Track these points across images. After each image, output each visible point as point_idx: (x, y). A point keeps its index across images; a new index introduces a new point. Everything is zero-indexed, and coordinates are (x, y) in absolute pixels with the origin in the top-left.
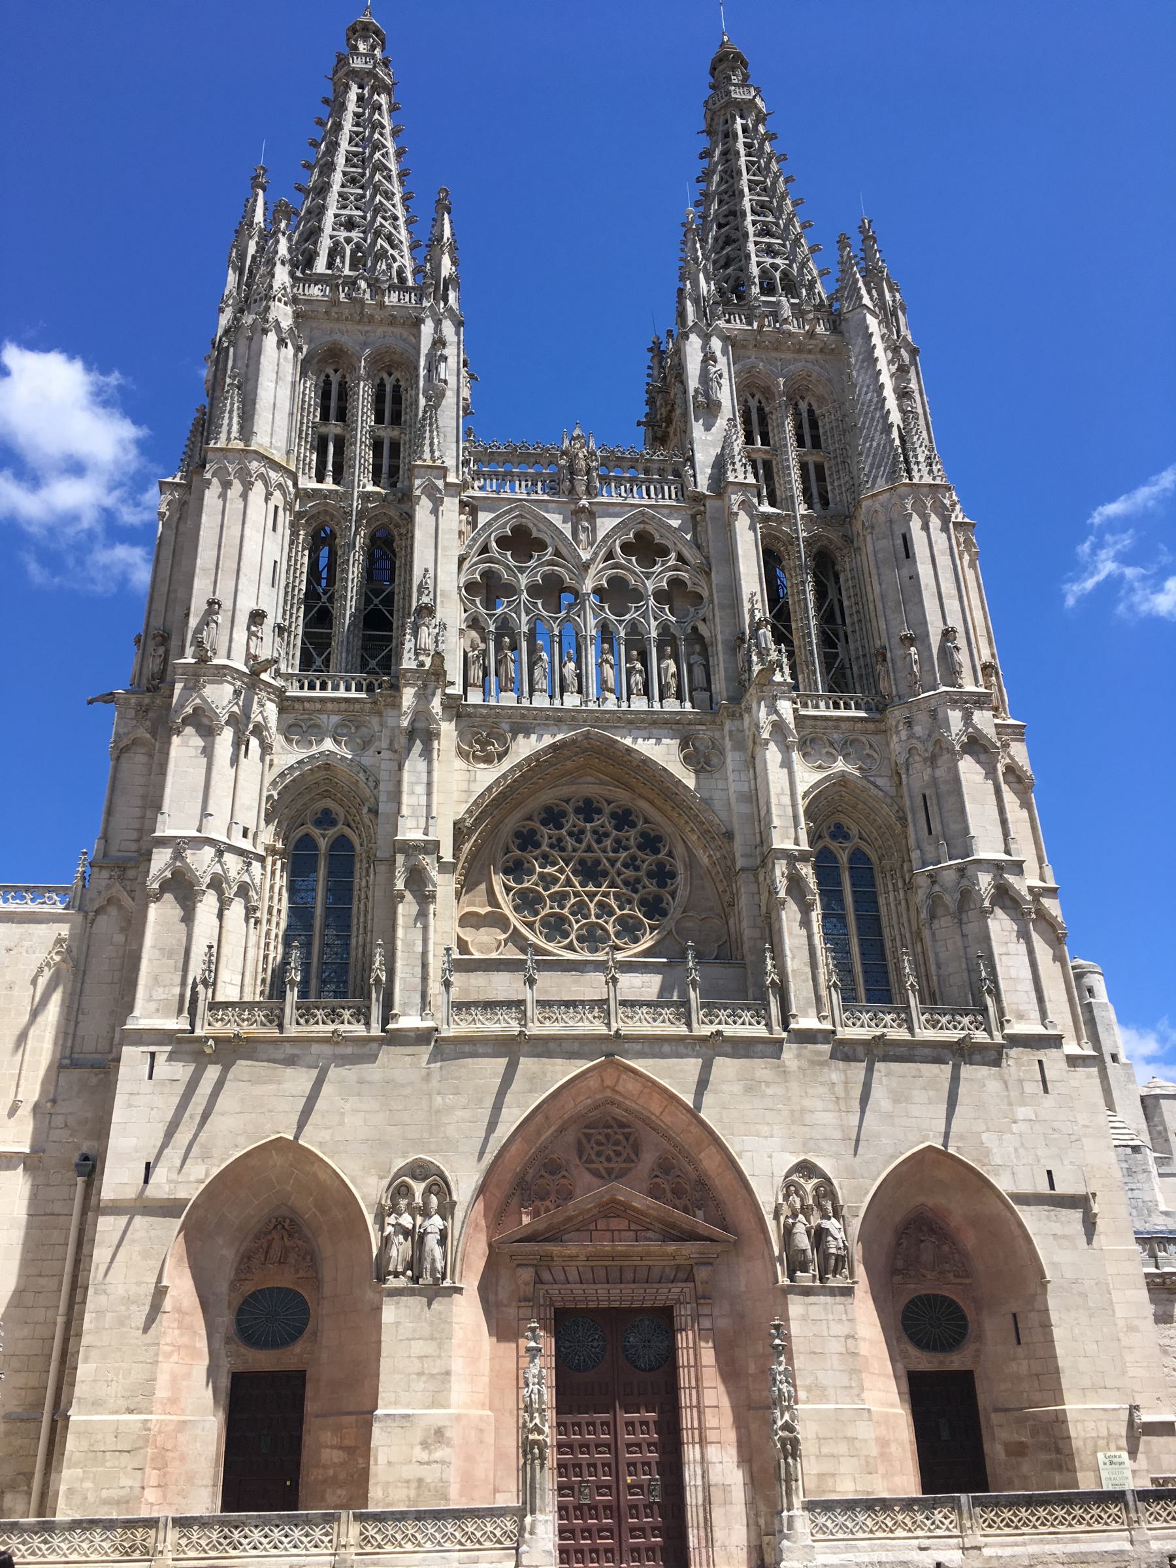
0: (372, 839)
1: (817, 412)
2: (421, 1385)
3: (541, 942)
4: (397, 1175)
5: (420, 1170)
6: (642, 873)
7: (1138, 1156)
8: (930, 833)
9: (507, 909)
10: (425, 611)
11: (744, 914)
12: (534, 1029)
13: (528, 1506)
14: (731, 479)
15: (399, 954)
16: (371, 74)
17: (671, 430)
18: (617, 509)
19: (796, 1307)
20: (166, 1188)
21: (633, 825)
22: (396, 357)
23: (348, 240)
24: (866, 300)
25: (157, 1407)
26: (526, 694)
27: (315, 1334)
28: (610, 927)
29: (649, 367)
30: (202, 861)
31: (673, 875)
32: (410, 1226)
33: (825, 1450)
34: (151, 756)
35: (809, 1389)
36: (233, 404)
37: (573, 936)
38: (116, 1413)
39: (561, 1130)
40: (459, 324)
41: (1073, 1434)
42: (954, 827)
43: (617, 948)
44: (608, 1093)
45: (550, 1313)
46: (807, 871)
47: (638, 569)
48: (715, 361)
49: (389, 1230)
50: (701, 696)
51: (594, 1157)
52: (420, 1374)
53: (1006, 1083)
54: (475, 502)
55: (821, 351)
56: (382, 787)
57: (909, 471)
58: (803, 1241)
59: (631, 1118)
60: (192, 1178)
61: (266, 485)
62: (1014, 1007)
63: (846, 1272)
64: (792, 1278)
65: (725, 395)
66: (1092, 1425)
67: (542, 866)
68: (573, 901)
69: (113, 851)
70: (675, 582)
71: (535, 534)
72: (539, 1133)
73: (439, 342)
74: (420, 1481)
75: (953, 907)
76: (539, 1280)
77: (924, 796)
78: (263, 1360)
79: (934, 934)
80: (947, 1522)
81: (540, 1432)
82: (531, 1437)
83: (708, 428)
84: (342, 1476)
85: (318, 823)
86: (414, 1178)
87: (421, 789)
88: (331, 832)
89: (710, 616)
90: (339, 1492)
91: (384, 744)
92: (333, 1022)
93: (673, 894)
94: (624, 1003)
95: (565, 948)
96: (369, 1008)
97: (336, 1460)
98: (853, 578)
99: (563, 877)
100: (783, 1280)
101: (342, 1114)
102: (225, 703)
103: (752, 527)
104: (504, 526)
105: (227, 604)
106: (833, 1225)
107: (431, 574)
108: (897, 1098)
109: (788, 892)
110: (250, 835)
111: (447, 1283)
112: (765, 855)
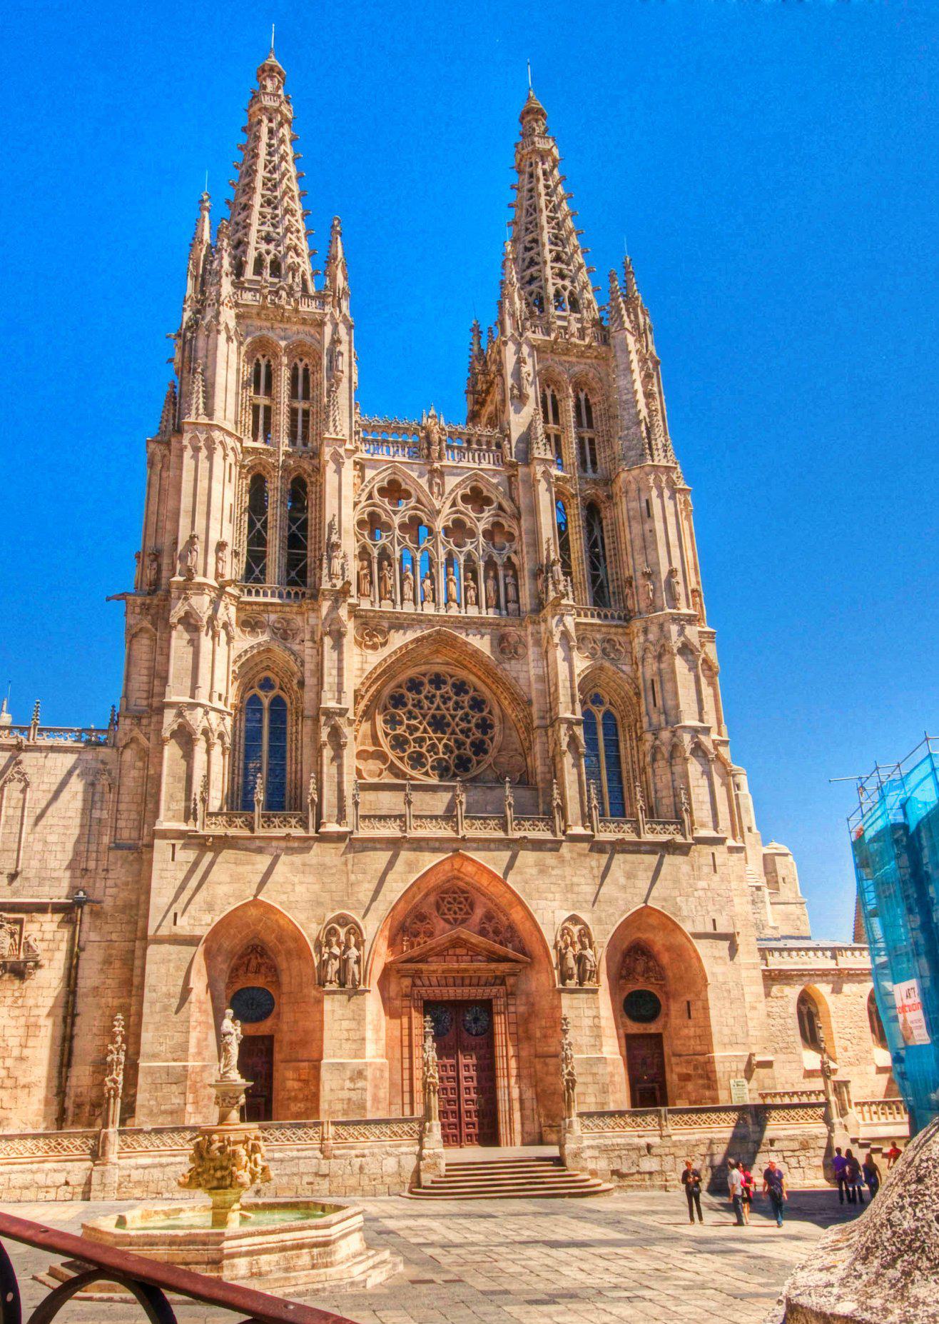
0: (300, 700)
2: (347, 1046)
3: (408, 770)
4: (329, 923)
5: (343, 920)
6: (472, 725)
8: (655, 705)
11: (538, 756)
13: (427, 1116)
14: (536, 456)
15: (325, 784)
16: (278, 110)
17: (489, 399)
18: (459, 471)
19: (566, 1000)
20: (188, 928)
21: (466, 692)
22: (306, 349)
23: (268, 252)
25: (190, 1058)
26: (399, 602)
27: (279, 1014)
29: (471, 344)
30: (197, 719)
31: (491, 727)
36: (198, 386)
37: (428, 767)
38: (167, 1061)
39: (427, 895)
40: (350, 328)
41: (717, 1069)
42: (670, 703)
44: (456, 872)
45: (420, 1003)
46: (579, 731)
47: (473, 515)
49: (326, 956)
51: (446, 911)
52: (347, 1040)
53: (693, 867)
55: (596, 357)
57: (652, 455)
58: (571, 963)
59: (469, 888)
60: (203, 923)
61: (224, 449)
63: (595, 979)
64: (563, 983)
65: (531, 391)
66: (728, 1064)
67: (408, 719)
68: (428, 743)
69: (132, 707)
70: (497, 525)
71: (404, 486)
73: (336, 341)
74: (349, 1099)
75: (666, 755)
76: (414, 985)
77: (652, 681)
79: (654, 771)
81: (434, 1077)
82: (428, 1080)
83: (518, 411)
84: (301, 1096)
85: (262, 687)
86: (339, 924)
87: (335, 672)
88: (272, 694)
91: (307, 637)
93: (492, 739)
95: (423, 774)
96: (307, 818)
98: (612, 524)
99: (422, 727)
100: (559, 986)
101: (293, 885)
102: (205, 609)
103: (549, 490)
104: (383, 480)
106: (589, 953)
107: (336, 519)
108: (630, 876)
109: (569, 745)
110: (223, 699)
111: (362, 987)
112: (552, 721)
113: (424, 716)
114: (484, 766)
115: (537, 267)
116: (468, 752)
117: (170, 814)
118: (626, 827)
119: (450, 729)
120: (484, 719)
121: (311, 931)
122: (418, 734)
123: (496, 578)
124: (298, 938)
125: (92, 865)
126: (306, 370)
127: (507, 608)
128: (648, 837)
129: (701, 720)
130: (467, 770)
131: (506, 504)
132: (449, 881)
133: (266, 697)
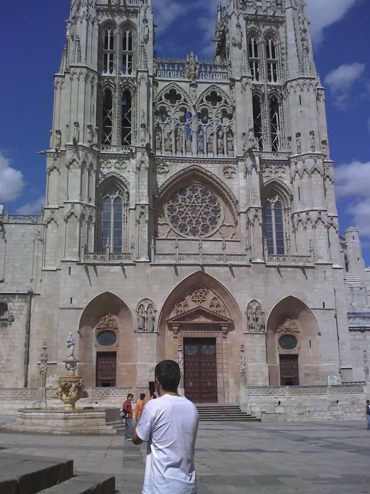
1: (275, 44)
7: (362, 291)
8: (300, 200)
9: (169, 223)
28: (199, 228)
31: (219, 211)
34: (60, 173)
43: (201, 234)
46: (260, 214)
47: (211, 106)
48: (240, 27)
50: (230, 152)
56: (131, 184)
68: (188, 219)
73: (145, 21)
80: (282, 392)
89: (234, 123)
93: (219, 217)
94: (203, 254)
99: (186, 212)
104: (167, 90)
105: (81, 123)
108: (282, 282)
111: (154, 332)
116: (208, 223)
118: (281, 259)
119: (200, 212)
120: (216, 207)
121: (132, 306)
122: (183, 215)
125: (34, 277)
126: (130, 34)
128: (293, 264)
130: (207, 232)
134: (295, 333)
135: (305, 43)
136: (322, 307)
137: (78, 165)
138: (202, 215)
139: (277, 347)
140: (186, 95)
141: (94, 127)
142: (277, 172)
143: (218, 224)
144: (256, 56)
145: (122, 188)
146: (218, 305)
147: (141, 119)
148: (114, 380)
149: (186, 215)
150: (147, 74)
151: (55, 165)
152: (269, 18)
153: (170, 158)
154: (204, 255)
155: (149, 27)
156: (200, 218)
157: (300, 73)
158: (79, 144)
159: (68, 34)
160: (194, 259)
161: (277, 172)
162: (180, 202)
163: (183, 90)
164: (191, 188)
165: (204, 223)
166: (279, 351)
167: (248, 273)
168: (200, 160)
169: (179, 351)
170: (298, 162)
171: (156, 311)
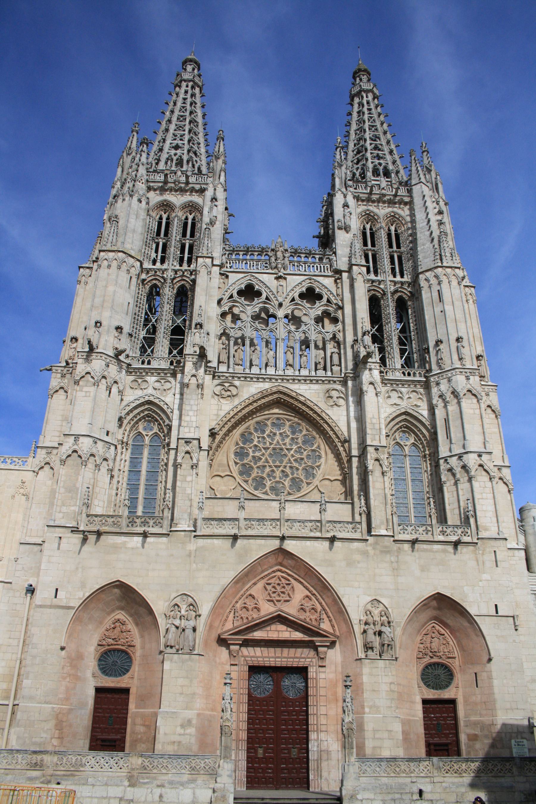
10: (198, 326)
12: (244, 533)
20: (65, 601)
23: (175, 154)
24: (423, 180)
28: (286, 483)
31: (320, 457)
32: (178, 625)
33: (377, 736)
35: (371, 707)
37: (267, 488)
43: (289, 494)
48: (348, 207)
50: (336, 369)
52: (182, 694)
54: (228, 274)
57: (441, 260)
60: (77, 597)
62: (484, 524)
64: (366, 656)
70: (326, 314)
72: (244, 584)
73: (214, 199)
74: (180, 742)
78: (110, 682)
80: (426, 770)
82: (224, 724)
84: (145, 738)
90: (143, 745)
92: (144, 525)
93: (318, 467)
94: (287, 520)
95: (264, 493)
97: (142, 731)
99: (264, 459)
108: (423, 569)
110: (110, 434)
113: (266, 449)
114: (311, 487)
115: (361, 154)
117: (61, 515)
118: (421, 529)
122: (260, 463)
123: (324, 349)
124: (150, 612)
126: (194, 219)
127: (331, 370)
128: (441, 538)
129: (485, 448)
130: (299, 489)
131: (333, 298)
132: (274, 572)
133: (147, 435)
134: (447, 660)
135: (442, 227)
136: (495, 614)
137: (92, 380)
138: (291, 463)
139: (417, 686)
140: (268, 291)
141: (127, 329)
142: (410, 398)
143: (316, 479)
144: (373, 245)
145: (162, 419)
146: (313, 609)
147: (197, 318)
148: (123, 740)
149: (264, 462)
150: (211, 260)
151: (62, 384)
152: (388, 197)
153: (239, 375)
154: (289, 523)
155: (219, 207)
156: (288, 468)
157: (436, 261)
158: (97, 351)
159: (106, 217)
160: (271, 527)
161: (410, 398)
162: (255, 443)
163: (265, 284)
164: (274, 421)
165: (295, 475)
166: (421, 692)
167: (365, 553)
168: (288, 378)
169: (225, 684)
170: (442, 381)
171: (200, 616)
